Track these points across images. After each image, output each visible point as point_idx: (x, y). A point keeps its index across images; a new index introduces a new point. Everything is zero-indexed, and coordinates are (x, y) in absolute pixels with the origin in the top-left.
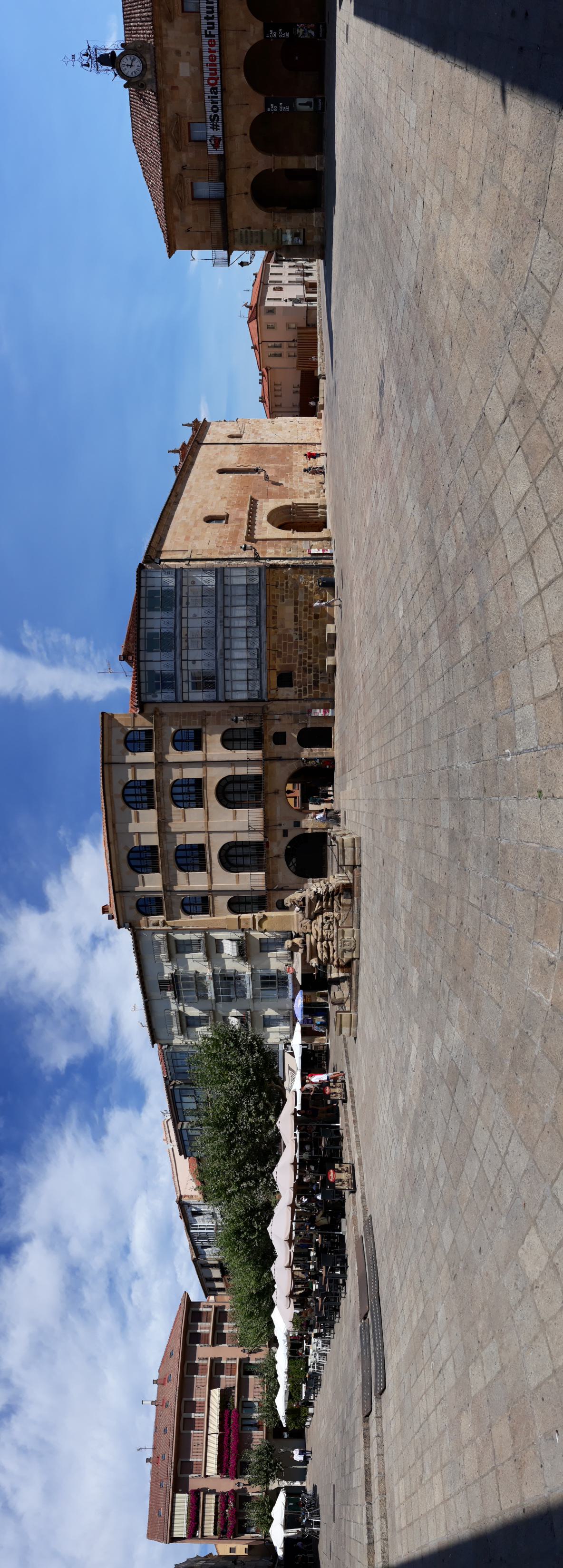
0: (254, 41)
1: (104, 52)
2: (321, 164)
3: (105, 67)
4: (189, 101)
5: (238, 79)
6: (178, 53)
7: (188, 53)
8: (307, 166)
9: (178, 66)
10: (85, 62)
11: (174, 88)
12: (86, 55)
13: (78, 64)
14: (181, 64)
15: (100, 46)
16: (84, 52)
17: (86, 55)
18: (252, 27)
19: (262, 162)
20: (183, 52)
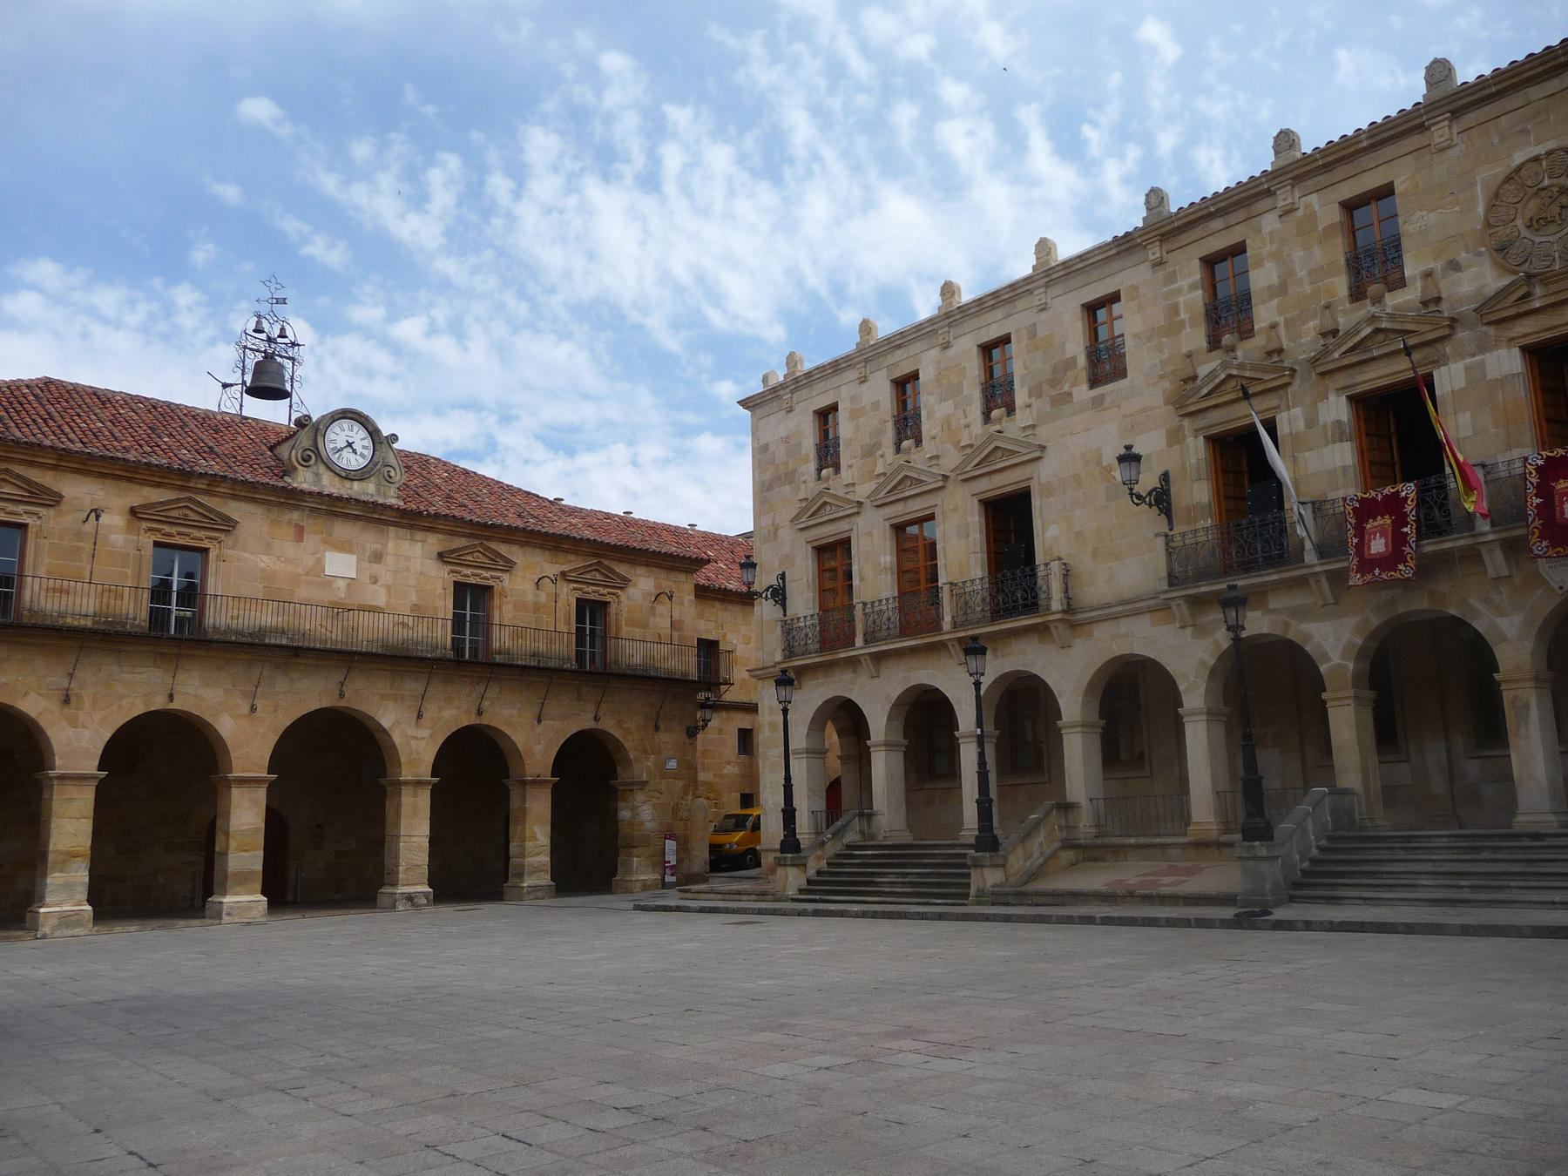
0: (397, 738)
1: (287, 377)
2: (66, 920)
3: (250, 365)
4: (264, 561)
5: (310, 694)
6: (378, 557)
7: (375, 580)
8: (54, 879)
9: (350, 552)
10: (265, 325)
11: (300, 534)
12: (282, 335)
13: (264, 309)
14: (353, 559)
15: (299, 371)
16: (289, 332)
17: (282, 335)
18: (426, 733)
19: (78, 739)
20: (377, 568)
